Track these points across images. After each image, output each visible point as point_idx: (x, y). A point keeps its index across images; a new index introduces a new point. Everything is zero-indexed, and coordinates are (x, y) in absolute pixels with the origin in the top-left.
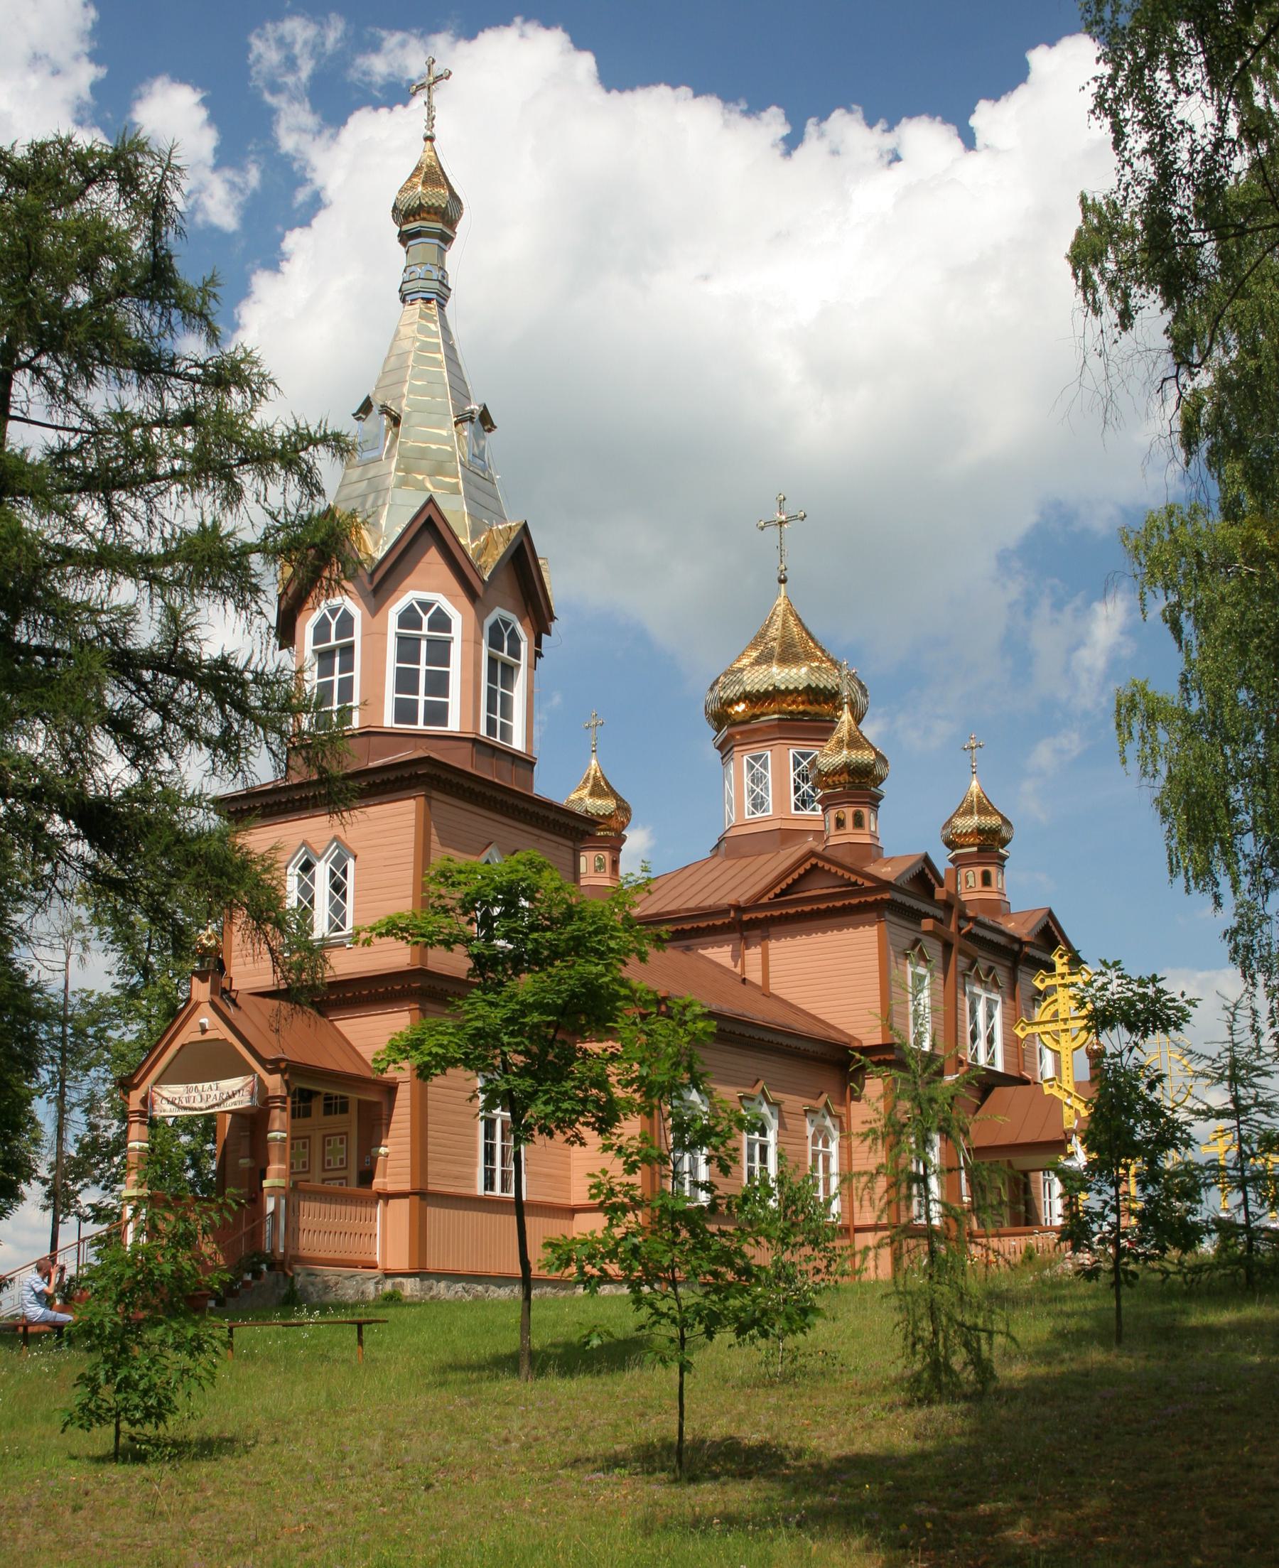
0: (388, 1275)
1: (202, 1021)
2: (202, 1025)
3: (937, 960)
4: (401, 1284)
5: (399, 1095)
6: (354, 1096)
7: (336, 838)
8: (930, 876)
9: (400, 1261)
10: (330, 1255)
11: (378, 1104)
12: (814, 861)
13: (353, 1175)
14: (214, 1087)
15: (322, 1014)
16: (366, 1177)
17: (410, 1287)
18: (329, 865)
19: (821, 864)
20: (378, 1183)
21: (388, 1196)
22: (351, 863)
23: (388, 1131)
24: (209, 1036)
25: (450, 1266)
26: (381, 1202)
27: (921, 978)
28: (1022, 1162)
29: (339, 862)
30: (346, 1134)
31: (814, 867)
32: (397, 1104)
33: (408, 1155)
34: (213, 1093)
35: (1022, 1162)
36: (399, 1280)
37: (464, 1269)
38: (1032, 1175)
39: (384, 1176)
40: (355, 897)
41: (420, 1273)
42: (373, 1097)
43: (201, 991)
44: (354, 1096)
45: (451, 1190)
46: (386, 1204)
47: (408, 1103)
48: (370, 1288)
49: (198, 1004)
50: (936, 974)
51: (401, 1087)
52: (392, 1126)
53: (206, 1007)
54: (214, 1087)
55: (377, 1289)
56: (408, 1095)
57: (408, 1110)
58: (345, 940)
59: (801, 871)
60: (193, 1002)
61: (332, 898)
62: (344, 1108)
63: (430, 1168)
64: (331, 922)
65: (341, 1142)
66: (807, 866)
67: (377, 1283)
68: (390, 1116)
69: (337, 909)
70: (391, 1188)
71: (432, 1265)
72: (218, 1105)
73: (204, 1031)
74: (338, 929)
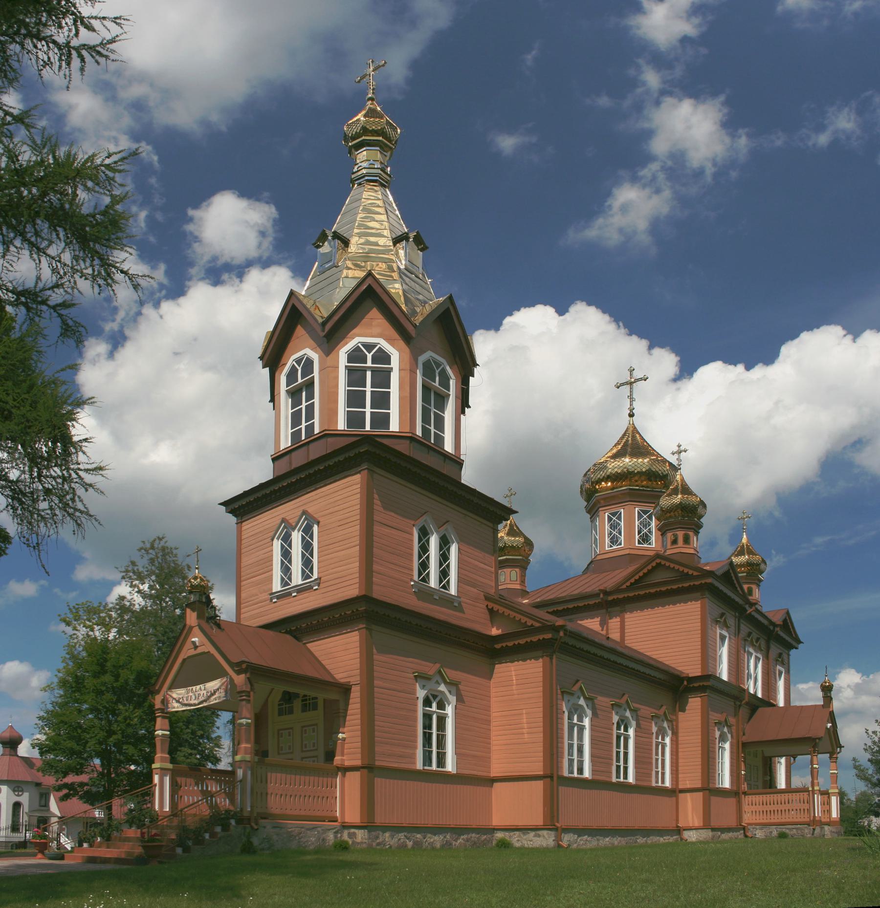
0: (345, 826)
1: (193, 640)
2: (194, 643)
3: (732, 629)
4: (354, 834)
5: (352, 695)
6: (321, 696)
7: (304, 512)
8: (732, 575)
9: (353, 815)
10: (297, 813)
11: (338, 701)
12: (658, 561)
13: (321, 753)
14: (203, 688)
15: (297, 639)
16: (330, 756)
17: (361, 835)
18: (301, 532)
19: (663, 562)
20: (338, 759)
21: (346, 770)
22: (315, 528)
23: (345, 721)
24: (199, 650)
25: (395, 819)
26: (340, 773)
27: (723, 638)
28: (768, 750)
29: (308, 530)
30: (316, 725)
31: (659, 565)
32: (351, 701)
33: (359, 739)
34: (202, 693)
35: (768, 750)
36: (353, 830)
37: (406, 821)
38: (773, 759)
39: (343, 755)
40: (318, 553)
41: (368, 825)
42: (333, 696)
43: (192, 618)
44: (321, 696)
45: (396, 765)
46: (344, 776)
47: (358, 700)
48: (331, 836)
49: (191, 628)
50: (732, 637)
51: (354, 689)
52: (348, 718)
53: (196, 630)
54: (203, 688)
55: (336, 837)
56: (358, 694)
57: (358, 706)
58: (312, 584)
59: (650, 567)
60: (187, 627)
61: (303, 555)
62: (315, 708)
63: (376, 749)
64: (303, 572)
65: (314, 731)
66: (654, 564)
67: (336, 833)
68: (346, 710)
69: (307, 563)
70: (347, 763)
71: (379, 820)
72: (205, 701)
73: (196, 647)
74: (308, 577)
